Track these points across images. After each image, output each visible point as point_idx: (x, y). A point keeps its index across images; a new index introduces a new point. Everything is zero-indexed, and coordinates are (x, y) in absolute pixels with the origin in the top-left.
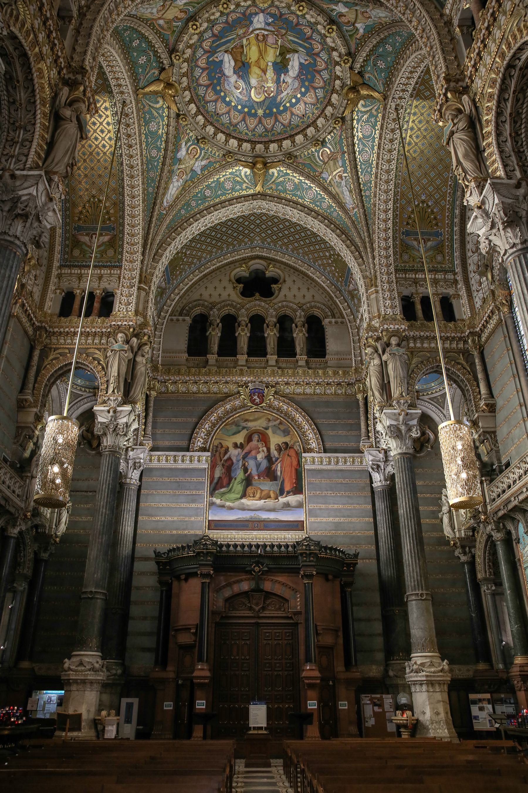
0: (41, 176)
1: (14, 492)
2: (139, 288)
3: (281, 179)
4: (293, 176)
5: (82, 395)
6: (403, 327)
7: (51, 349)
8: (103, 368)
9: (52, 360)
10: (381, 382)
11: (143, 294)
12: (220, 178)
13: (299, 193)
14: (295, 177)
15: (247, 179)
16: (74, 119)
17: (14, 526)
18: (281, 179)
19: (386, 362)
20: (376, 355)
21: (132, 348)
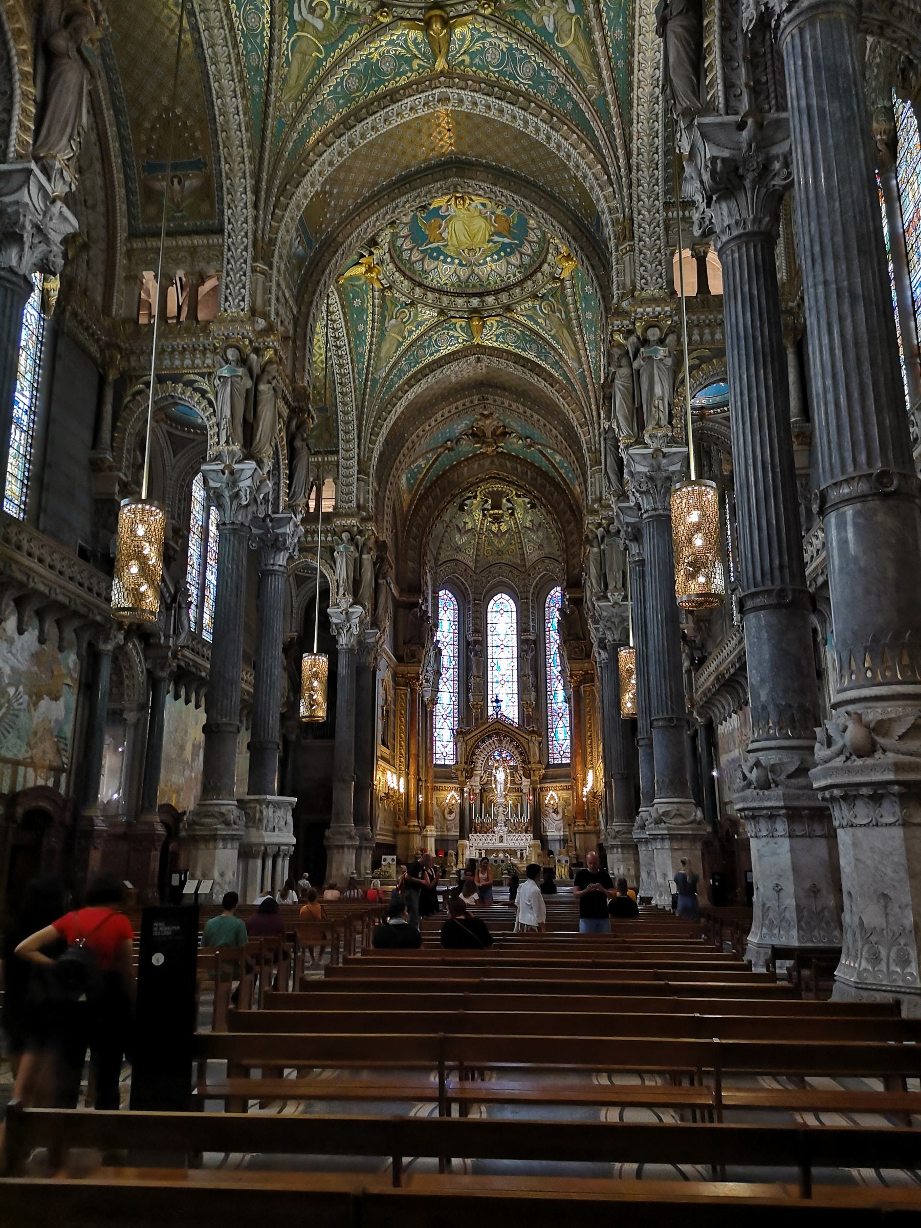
0: (30, 171)
1: (99, 595)
2: (254, 270)
3: (478, 45)
4: (497, 37)
5: (193, 440)
6: (667, 309)
7: (130, 377)
8: (210, 403)
9: (134, 395)
10: (630, 402)
11: (261, 278)
12: (371, 53)
13: (508, 68)
14: (501, 39)
15: (419, 50)
16: (73, 53)
17: (107, 639)
18: (478, 45)
19: (639, 371)
20: (624, 362)
21: (250, 371)
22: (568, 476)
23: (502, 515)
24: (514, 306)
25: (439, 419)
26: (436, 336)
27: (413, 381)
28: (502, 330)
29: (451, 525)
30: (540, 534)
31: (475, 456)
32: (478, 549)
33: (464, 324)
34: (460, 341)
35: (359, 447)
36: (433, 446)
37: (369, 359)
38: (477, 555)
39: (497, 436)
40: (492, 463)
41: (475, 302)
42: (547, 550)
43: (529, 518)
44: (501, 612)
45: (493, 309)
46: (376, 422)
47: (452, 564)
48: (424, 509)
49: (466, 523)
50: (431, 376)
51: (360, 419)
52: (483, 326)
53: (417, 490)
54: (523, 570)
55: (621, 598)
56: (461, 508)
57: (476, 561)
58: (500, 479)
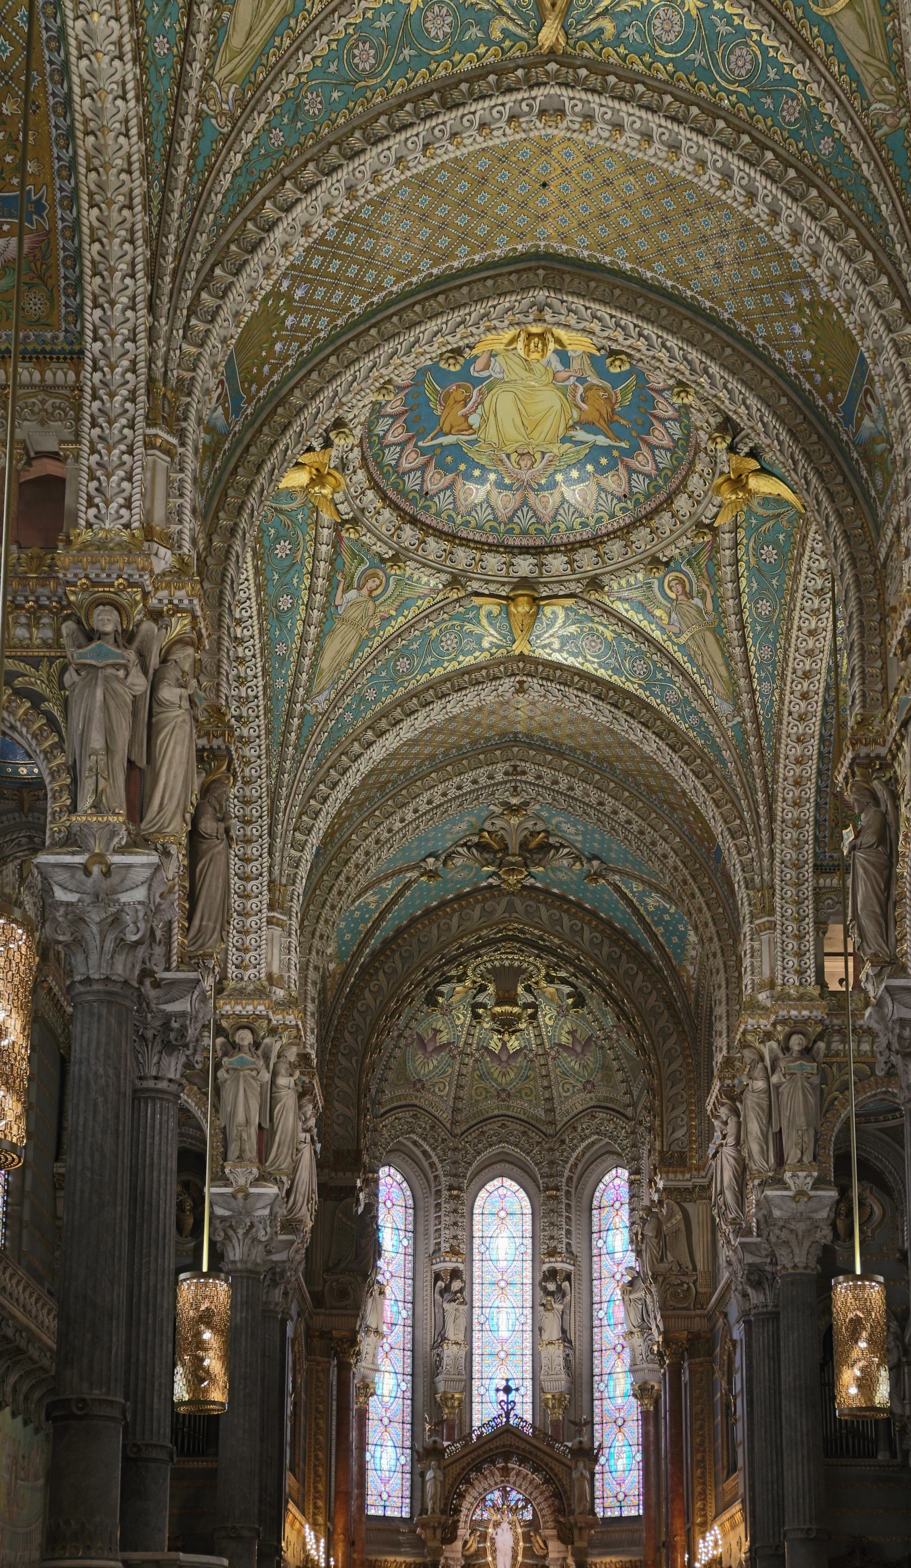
23: (519, 1017)
24: (605, 579)
25: (424, 808)
26: (435, 632)
27: (384, 724)
28: (573, 629)
29: (407, 1033)
30: (589, 1058)
31: (477, 890)
32: (460, 1087)
33: (496, 610)
34: (486, 644)
35: (270, 854)
36: (399, 864)
37: (298, 671)
38: (457, 1098)
39: (530, 851)
40: (510, 907)
41: (524, 566)
42: (602, 1091)
44: (503, 1215)
45: (561, 582)
46: (305, 804)
47: (407, 1115)
49: (437, 1031)
50: (421, 714)
51: (274, 796)
52: (535, 616)
53: (356, 955)
54: (550, 1131)
55: (810, 1181)
56: (431, 1000)
57: (455, 1110)
58: (525, 942)
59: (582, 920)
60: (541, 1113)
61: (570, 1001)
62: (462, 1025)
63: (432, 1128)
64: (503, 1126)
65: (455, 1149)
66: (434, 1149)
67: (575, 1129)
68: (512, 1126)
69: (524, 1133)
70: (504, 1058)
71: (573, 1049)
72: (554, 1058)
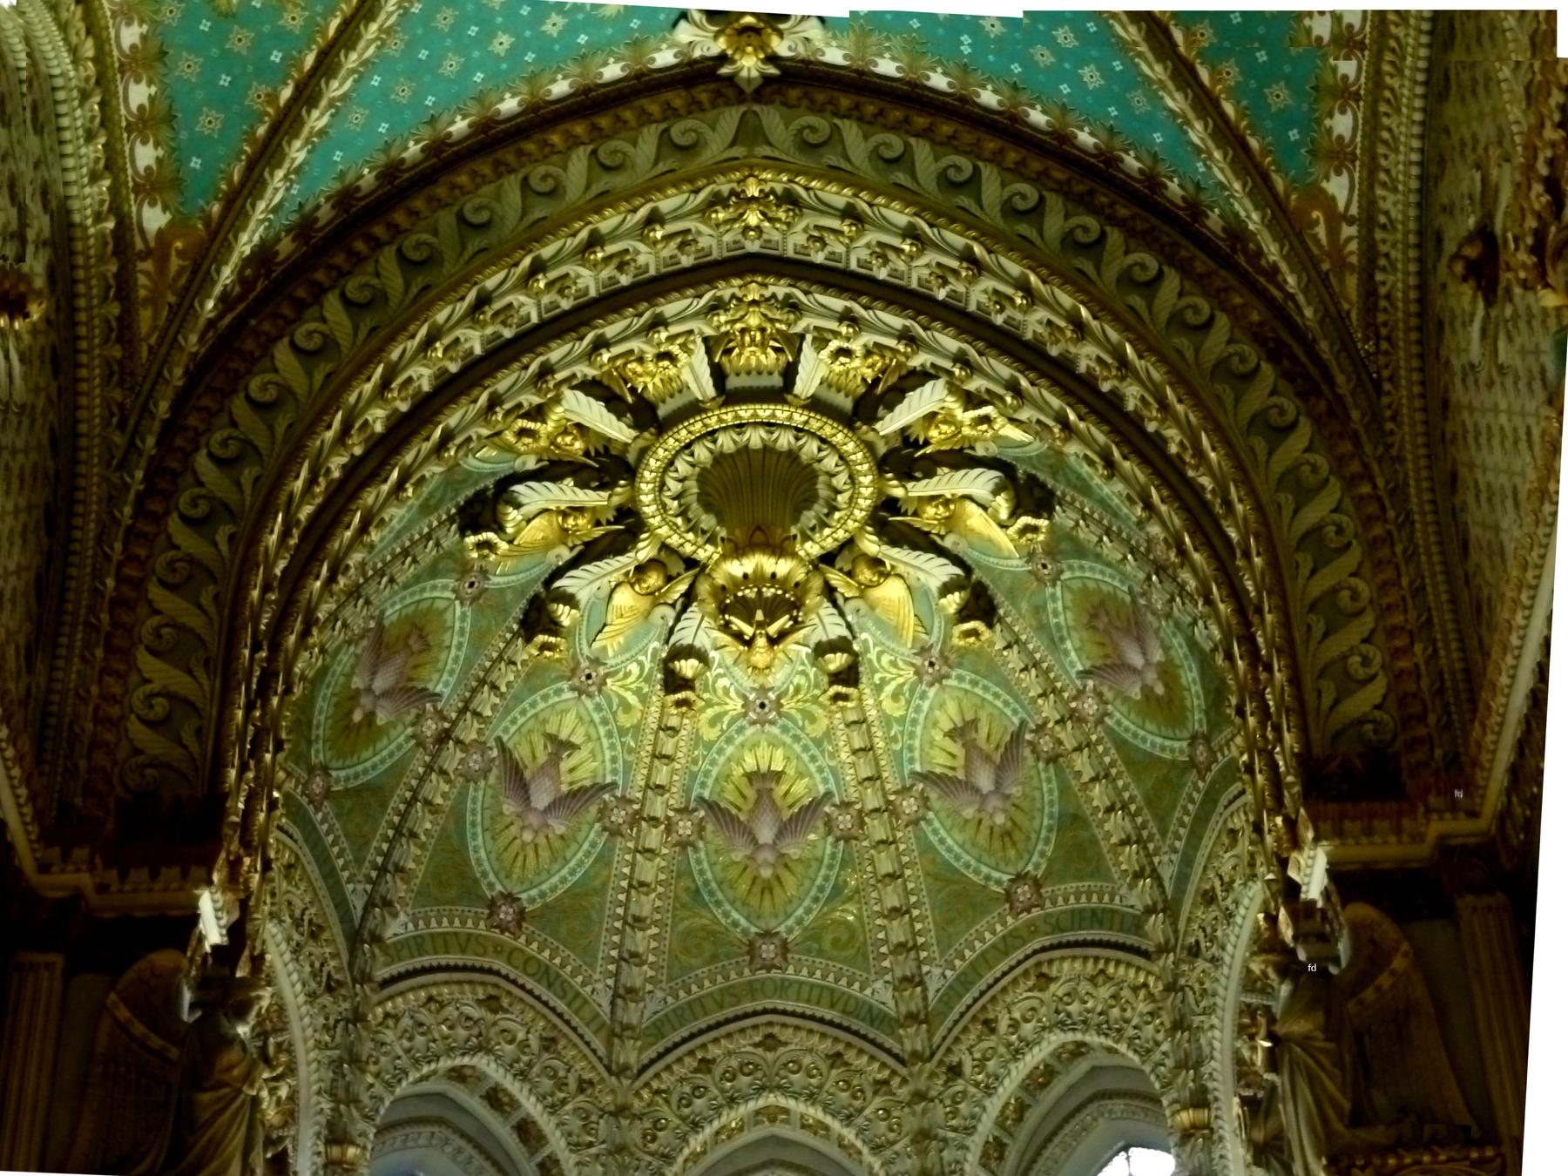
22: (1256, 107)
29: (469, 731)
42: (1067, 896)
43: (949, 716)
47: (466, 1001)
48: (282, 354)
49: (561, 746)
54: (913, 1039)
59: (973, 152)
60: (881, 994)
61: (953, 601)
62: (637, 729)
63: (548, 1044)
64: (770, 1042)
65: (621, 1111)
66: (553, 1109)
67: (990, 1026)
68: (796, 1041)
69: (836, 1059)
70: (766, 834)
71: (969, 786)
72: (915, 822)
